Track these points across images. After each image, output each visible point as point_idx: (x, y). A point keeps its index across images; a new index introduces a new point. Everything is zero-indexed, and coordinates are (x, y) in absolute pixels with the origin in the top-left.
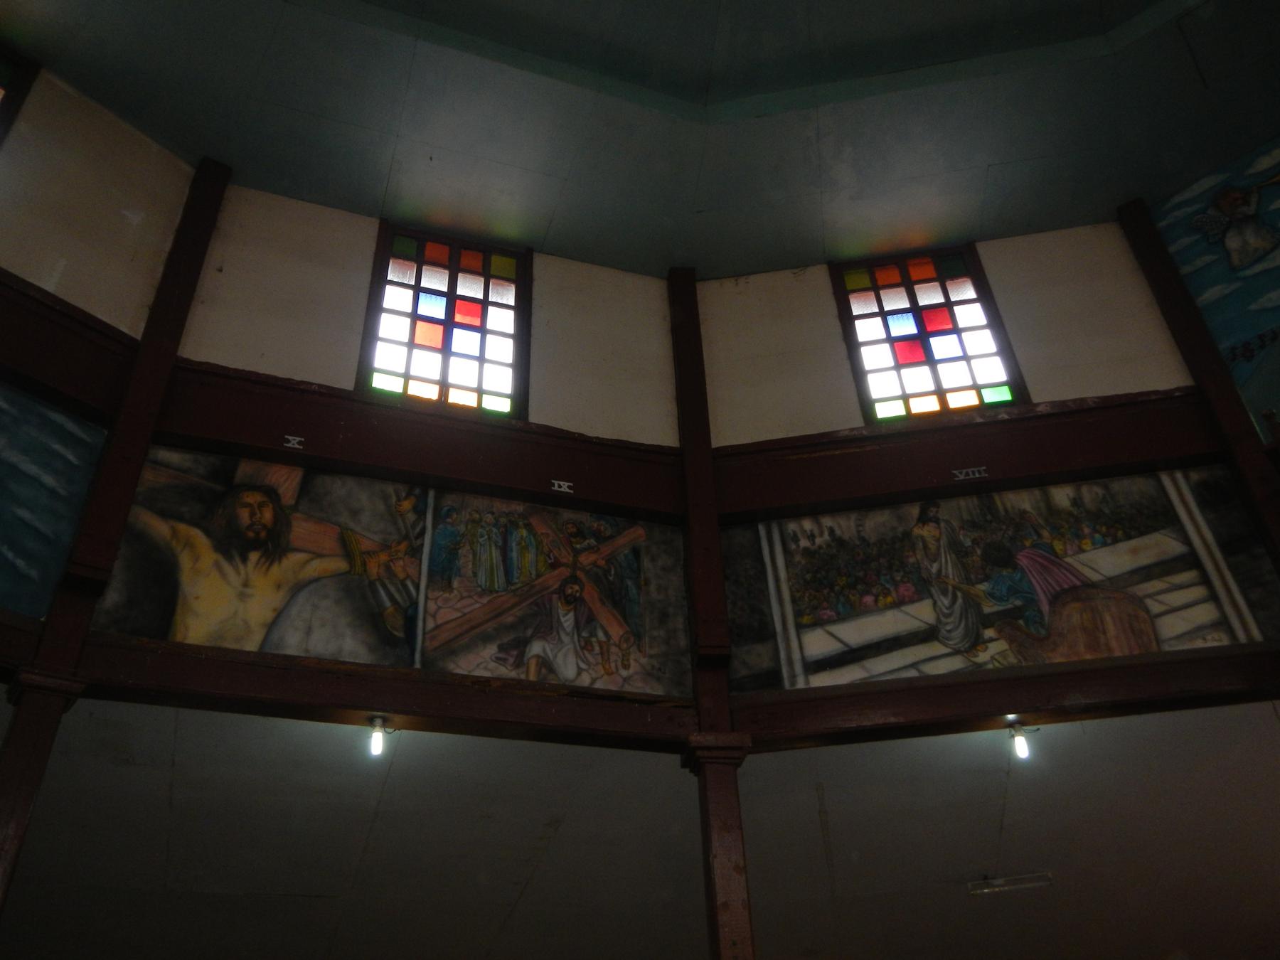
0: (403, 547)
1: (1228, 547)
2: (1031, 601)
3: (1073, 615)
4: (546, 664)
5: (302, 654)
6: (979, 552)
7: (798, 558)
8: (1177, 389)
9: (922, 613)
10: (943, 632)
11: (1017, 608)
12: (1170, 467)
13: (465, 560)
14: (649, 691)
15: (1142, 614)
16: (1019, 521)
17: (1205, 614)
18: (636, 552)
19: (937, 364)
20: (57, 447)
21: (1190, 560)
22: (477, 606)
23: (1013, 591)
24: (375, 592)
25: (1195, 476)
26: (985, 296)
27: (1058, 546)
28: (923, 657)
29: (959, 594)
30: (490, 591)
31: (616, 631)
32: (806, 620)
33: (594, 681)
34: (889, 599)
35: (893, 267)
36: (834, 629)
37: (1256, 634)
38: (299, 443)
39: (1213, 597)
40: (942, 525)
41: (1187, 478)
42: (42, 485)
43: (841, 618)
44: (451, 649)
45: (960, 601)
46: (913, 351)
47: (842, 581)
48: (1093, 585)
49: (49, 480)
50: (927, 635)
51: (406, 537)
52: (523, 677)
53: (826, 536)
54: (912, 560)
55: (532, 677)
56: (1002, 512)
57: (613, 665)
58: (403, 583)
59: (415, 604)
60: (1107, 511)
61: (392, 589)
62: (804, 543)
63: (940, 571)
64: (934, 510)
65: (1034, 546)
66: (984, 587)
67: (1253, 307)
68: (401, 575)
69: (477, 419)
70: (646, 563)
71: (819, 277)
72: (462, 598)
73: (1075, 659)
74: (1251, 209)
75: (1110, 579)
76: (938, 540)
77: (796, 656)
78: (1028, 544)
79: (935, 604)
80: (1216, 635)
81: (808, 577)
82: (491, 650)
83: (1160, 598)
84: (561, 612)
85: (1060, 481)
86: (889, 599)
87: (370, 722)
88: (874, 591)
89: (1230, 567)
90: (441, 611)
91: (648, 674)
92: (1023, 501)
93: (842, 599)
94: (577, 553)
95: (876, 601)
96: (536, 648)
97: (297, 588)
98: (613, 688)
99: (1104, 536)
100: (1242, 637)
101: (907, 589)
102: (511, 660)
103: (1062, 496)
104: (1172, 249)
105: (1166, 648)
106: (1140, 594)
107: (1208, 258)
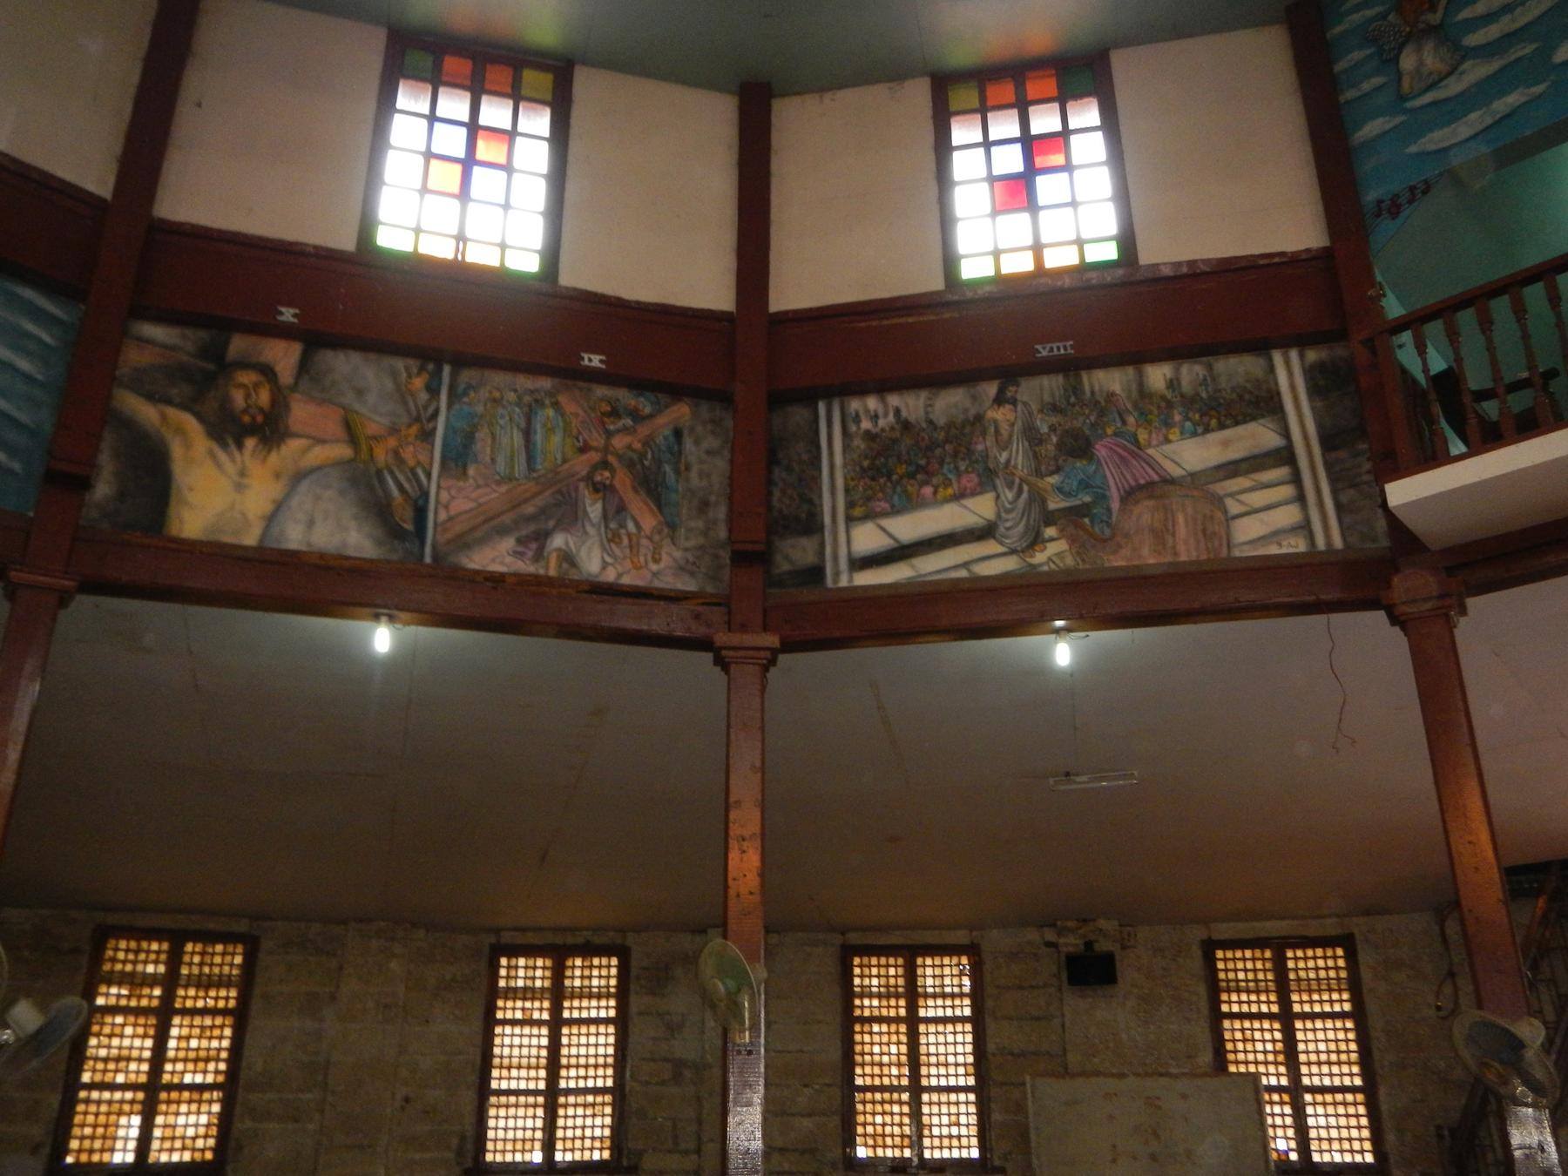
0: (414, 430)
1: (1329, 441)
2: (1102, 498)
3: (1144, 513)
4: (567, 558)
5: (304, 548)
6: (1055, 439)
7: (858, 443)
8: (1308, 251)
9: (981, 508)
10: (1002, 529)
11: (1086, 505)
12: (1285, 345)
13: (482, 445)
14: (680, 586)
15: (1219, 515)
16: (1104, 406)
17: (1288, 516)
18: (678, 434)
19: (1036, 208)
20: (30, 327)
21: (1285, 456)
22: (495, 495)
23: (1085, 485)
24: (382, 481)
25: (1312, 355)
26: (1110, 124)
27: (1142, 436)
28: (975, 555)
29: (1026, 488)
30: (510, 478)
31: (649, 522)
32: (857, 512)
33: (620, 576)
34: (950, 491)
35: (1007, 80)
36: (885, 522)
37: (1338, 543)
38: (295, 316)
39: (1301, 498)
40: (1020, 407)
41: (1302, 356)
42: (15, 370)
43: (896, 511)
44: (464, 542)
45: (1025, 495)
46: (1017, 191)
47: (902, 469)
48: (1170, 481)
49: (24, 364)
51: (418, 419)
52: (542, 572)
53: (891, 418)
54: (980, 447)
55: (552, 572)
56: (1088, 394)
57: (642, 559)
58: (413, 470)
59: (426, 495)
60: (1204, 395)
61: (401, 478)
62: (866, 425)
63: (1008, 461)
64: (1012, 389)
65: (1116, 434)
66: (1053, 480)
67: (1413, 149)
68: (411, 463)
69: (496, 283)
70: (688, 444)
71: (919, 92)
72: (478, 487)
73: (1136, 562)
74: (1435, 18)
75: (1192, 475)
76: (1013, 425)
77: (843, 552)
78: (1109, 431)
79: (998, 497)
80: (1293, 542)
81: (866, 463)
82: (509, 543)
83: (1243, 497)
84: (588, 501)
85: (1156, 359)
86: (950, 491)
87: (377, 617)
88: (935, 481)
89: (1328, 466)
90: (453, 501)
91: (682, 569)
92: (1112, 381)
93: (899, 489)
94: (609, 434)
95: (935, 493)
96: (558, 541)
97: (299, 477)
98: (640, 583)
99: (1195, 424)
100: (1321, 544)
101: (970, 481)
102: (530, 554)
103: (1158, 375)
105: (1237, 553)
106: (1221, 493)
107: (1377, 81)
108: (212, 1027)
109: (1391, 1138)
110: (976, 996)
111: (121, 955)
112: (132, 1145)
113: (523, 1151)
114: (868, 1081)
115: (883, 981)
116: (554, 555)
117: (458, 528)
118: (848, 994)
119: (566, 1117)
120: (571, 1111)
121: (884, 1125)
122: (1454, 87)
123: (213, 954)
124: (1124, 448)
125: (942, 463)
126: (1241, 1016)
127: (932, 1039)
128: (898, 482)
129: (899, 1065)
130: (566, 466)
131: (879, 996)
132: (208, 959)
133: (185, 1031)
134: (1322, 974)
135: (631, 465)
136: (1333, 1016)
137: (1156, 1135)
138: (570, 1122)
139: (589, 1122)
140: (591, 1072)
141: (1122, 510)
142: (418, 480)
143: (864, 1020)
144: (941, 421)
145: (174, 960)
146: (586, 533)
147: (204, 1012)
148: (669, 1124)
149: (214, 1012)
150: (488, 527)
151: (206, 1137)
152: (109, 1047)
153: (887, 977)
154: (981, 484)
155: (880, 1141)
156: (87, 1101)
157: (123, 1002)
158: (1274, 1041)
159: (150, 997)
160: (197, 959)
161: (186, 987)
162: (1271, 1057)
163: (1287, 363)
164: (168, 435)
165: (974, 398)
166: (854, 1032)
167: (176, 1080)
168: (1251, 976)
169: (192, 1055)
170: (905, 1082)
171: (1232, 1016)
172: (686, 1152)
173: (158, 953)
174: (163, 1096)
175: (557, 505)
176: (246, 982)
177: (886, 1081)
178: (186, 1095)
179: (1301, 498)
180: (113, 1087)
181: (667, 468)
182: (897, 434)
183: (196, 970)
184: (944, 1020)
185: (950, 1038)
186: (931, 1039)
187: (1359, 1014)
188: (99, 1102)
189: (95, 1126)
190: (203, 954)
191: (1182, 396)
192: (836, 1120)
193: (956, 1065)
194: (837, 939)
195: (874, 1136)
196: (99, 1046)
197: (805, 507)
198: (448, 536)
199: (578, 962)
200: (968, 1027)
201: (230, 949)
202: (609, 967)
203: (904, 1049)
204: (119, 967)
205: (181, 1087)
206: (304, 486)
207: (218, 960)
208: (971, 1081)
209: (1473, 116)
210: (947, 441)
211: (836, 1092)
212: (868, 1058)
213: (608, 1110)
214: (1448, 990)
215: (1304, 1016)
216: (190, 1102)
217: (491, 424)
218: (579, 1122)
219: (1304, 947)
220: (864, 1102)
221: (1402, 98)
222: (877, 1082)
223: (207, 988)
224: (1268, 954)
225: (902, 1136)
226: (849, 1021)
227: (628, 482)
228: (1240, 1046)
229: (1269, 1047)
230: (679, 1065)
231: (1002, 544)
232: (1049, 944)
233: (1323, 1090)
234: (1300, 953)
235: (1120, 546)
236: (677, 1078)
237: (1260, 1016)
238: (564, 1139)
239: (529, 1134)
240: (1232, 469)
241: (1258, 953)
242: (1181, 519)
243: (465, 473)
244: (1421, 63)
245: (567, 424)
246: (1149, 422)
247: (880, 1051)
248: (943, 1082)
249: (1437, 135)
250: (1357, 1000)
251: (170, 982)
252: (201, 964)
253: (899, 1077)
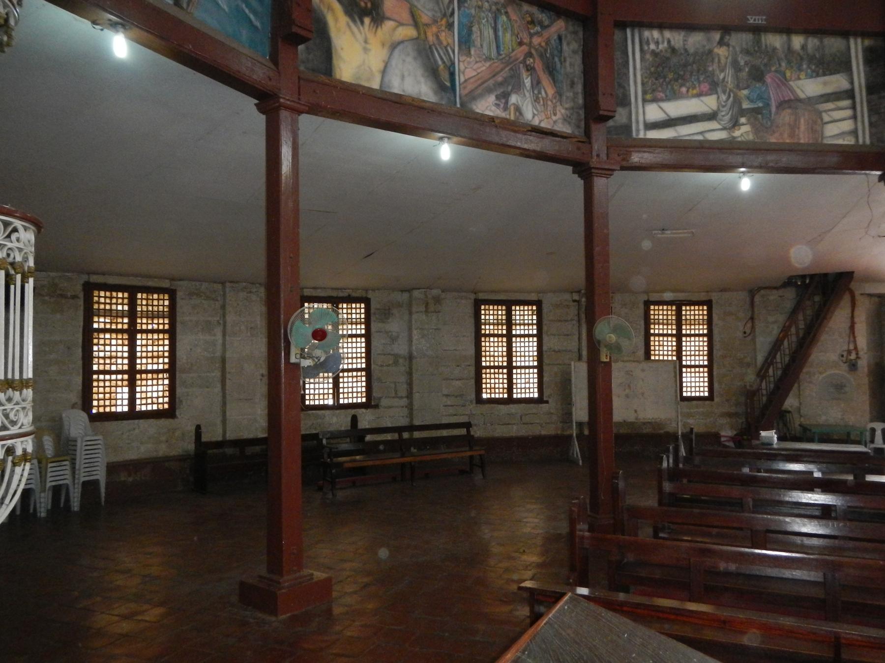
0: (444, 22)
1: (871, 89)
2: (767, 105)
3: (786, 116)
4: (518, 109)
6: (747, 70)
7: (648, 56)
9: (709, 103)
10: (719, 116)
11: (759, 108)
12: (856, 35)
13: (476, 36)
14: (564, 130)
16: (771, 53)
17: (848, 126)
18: (560, 38)
21: (850, 94)
22: (484, 68)
23: (760, 98)
24: (432, 52)
25: (867, 42)
27: (788, 74)
28: (707, 129)
30: (488, 58)
31: (551, 91)
32: (648, 97)
34: (695, 92)
37: (868, 141)
39: (854, 117)
40: (731, 49)
41: (863, 42)
44: (473, 96)
45: (731, 99)
47: (671, 76)
48: (799, 100)
50: (712, 116)
51: (445, 15)
52: (508, 117)
53: (666, 44)
54: (710, 69)
55: (512, 118)
56: (764, 46)
58: (446, 48)
59: (453, 64)
61: (442, 54)
62: (652, 46)
63: (724, 78)
64: (727, 37)
65: (776, 71)
68: (445, 43)
70: (565, 47)
72: (477, 62)
73: (781, 141)
75: (809, 98)
76: (727, 58)
77: (641, 118)
79: (718, 98)
81: (652, 69)
82: (492, 98)
83: (830, 113)
84: (525, 76)
86: (695, 92)
88: (688, 84)
89: (869, 102)
90: (469, 70)
91: (566, 120)
92: (775, 41)
93: (669, 87)
94: (531, 36)
95: (688, 91)
96: (514, 99)
97: (394, 46)
99: (813, 71)
100: (861, 141)
102: (502, 106)
103: (797, 41)
105: (825, 142)
108: (158, 339)
109: (716, 385)
110: (539, 324)
111: (102, 300)
112: (126, 402)
113: (324, 399)
114: (488, 364)
115: (496, 317)
116: (512, 108)
117: (470, 87)
118: (478, 323)
119: (344, 382)
120: (346, 379)
121: (495, 383)
123: (153, 300)
124: (780, 80)
125: (691, 75)
126: (659, 335)
127: (518, 344)
128: (669, 83)
129: (503, 356)
130: (514, 53)
131: (494, 324)
132: (150, 302)
133: (144, 342)
134: (697, 317)
135: (541, 56)
136: (699, 335)
137: (629, 386)
138: (346, 385)
139: (355, 385)
140: (354, 361)
141: (777, 113)
142: (449, 55)
143: (486, 336)
144: (692, 50)
145: (133, 303)
146: (525, 95)
147: (153, 331)
148: (393, 385)
149: (158, 331)
150: (481, 90)
151: (163, 397)
152: (105, 351)
153: (498, 315)
154: (710, 89)
155: (493, 391)
156: (98, 380)
157: (108, 326)
158: (672, 346)
159: (123, 323)
160: (144, 302)
161: (141, 318)
162: (670, 353)
163: (856, 44)
164: (325, 11)
165: (709, 40)
166: (481, 341)
167: (143, 368)
168: (665, 317)
169: (150, 354)
170: (505, 364)
171: (655, 335)
172: (401, 398)
173: (123, 298)
174: (138, 376)
175: (512, 77)
176: (172, 314)
177: (496, 364)
178: (150, 376)
180: (110, 372)
181: (556, 59)
182: (668, 55)
183: (145, 308)
184: (524, 336)
185: (527, 344)
186: (517, 343)
187: (710, 335)
188: (104, 381)
189: (104, 393)
190: (147, 299)
191: (808, 55)
192: (473, 382)
193: (529, 356)
194: (473, 296)
195: (490, 388)
196: (99, 351)
197: (622, 90)
198: (466, 91)
199: (345, 306)
200: (535, 339)
201: (161, 297)
202: (360, 308)
203: (505, 349)
204: (102, 306)
205: (147, 372)
206: (397, 52)
207: (155, 303)
208: (536, 364)
210: (694, 62)
211: (472, 369)
212: (488, 353)
213: (364, 379)
214: (749, 325)
215: (687, 335)
216: (152, 379)
217: (479, 23)
218: (350, 385)
219: (690, 305)
220: (486, 374)
222: (492, 364)
223: (153, 318)
224: (674, 308)
225: (503, 388)
226: (478, 336)
227: (540, 65)
228: (657, 348)
229: (670, 348)
230: (396, 357)
231: (719, 124)
232: (574, 301)
233: (691, 367)
234: (688, 308)
235: (774, 132)
236: (396, 363)
237: (667, 335)
238: (343, 393)
239: (326, 391)
240: (827, 98)
241: (669, 308)
242: (802, 121)
243: (470, 53)
245: (512, 26)
246: (792, 67)
247: (493, 351)
248: (523, 364)
250: (710, 329)
251: (132, 314)
252: (147, 305)
253: (503, 362)
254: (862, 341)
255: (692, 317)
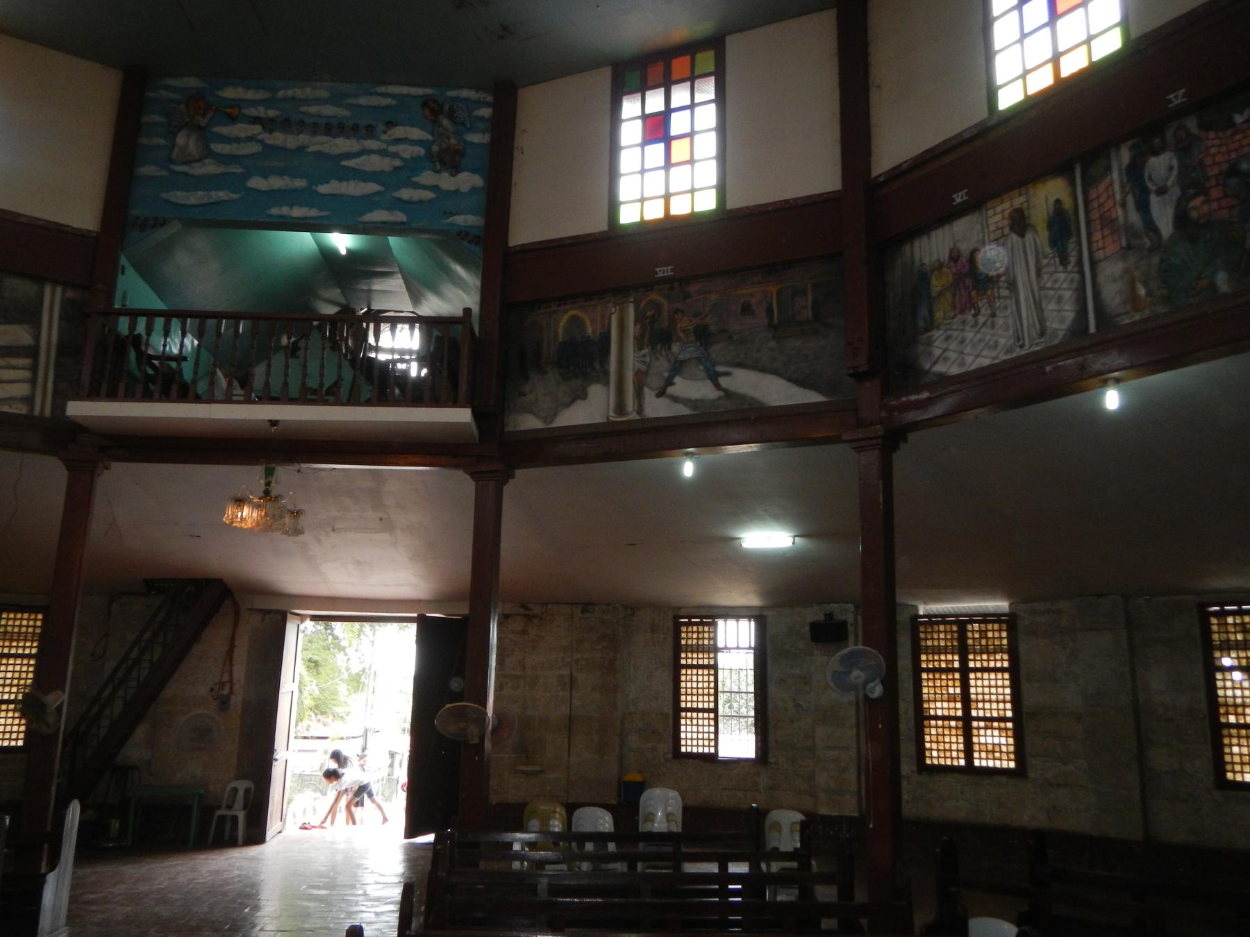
12: (55, 282)
17: (22, 390)
25: (70, 294)
37: (48, 413)
39: (33, 382)
41: (64, 292)
67: (164, 195)
74: (203, 122)
100: (37, 412)
104: (145, 119)
122: (197, 170)
163: (53, 293)
179: (33, 382)
209: (200, 193)
219: (16, 612)
221: (171, 161)
244: (187, 145)
249: (179, 194)
254: (240, 672)
255: (16, 630)
